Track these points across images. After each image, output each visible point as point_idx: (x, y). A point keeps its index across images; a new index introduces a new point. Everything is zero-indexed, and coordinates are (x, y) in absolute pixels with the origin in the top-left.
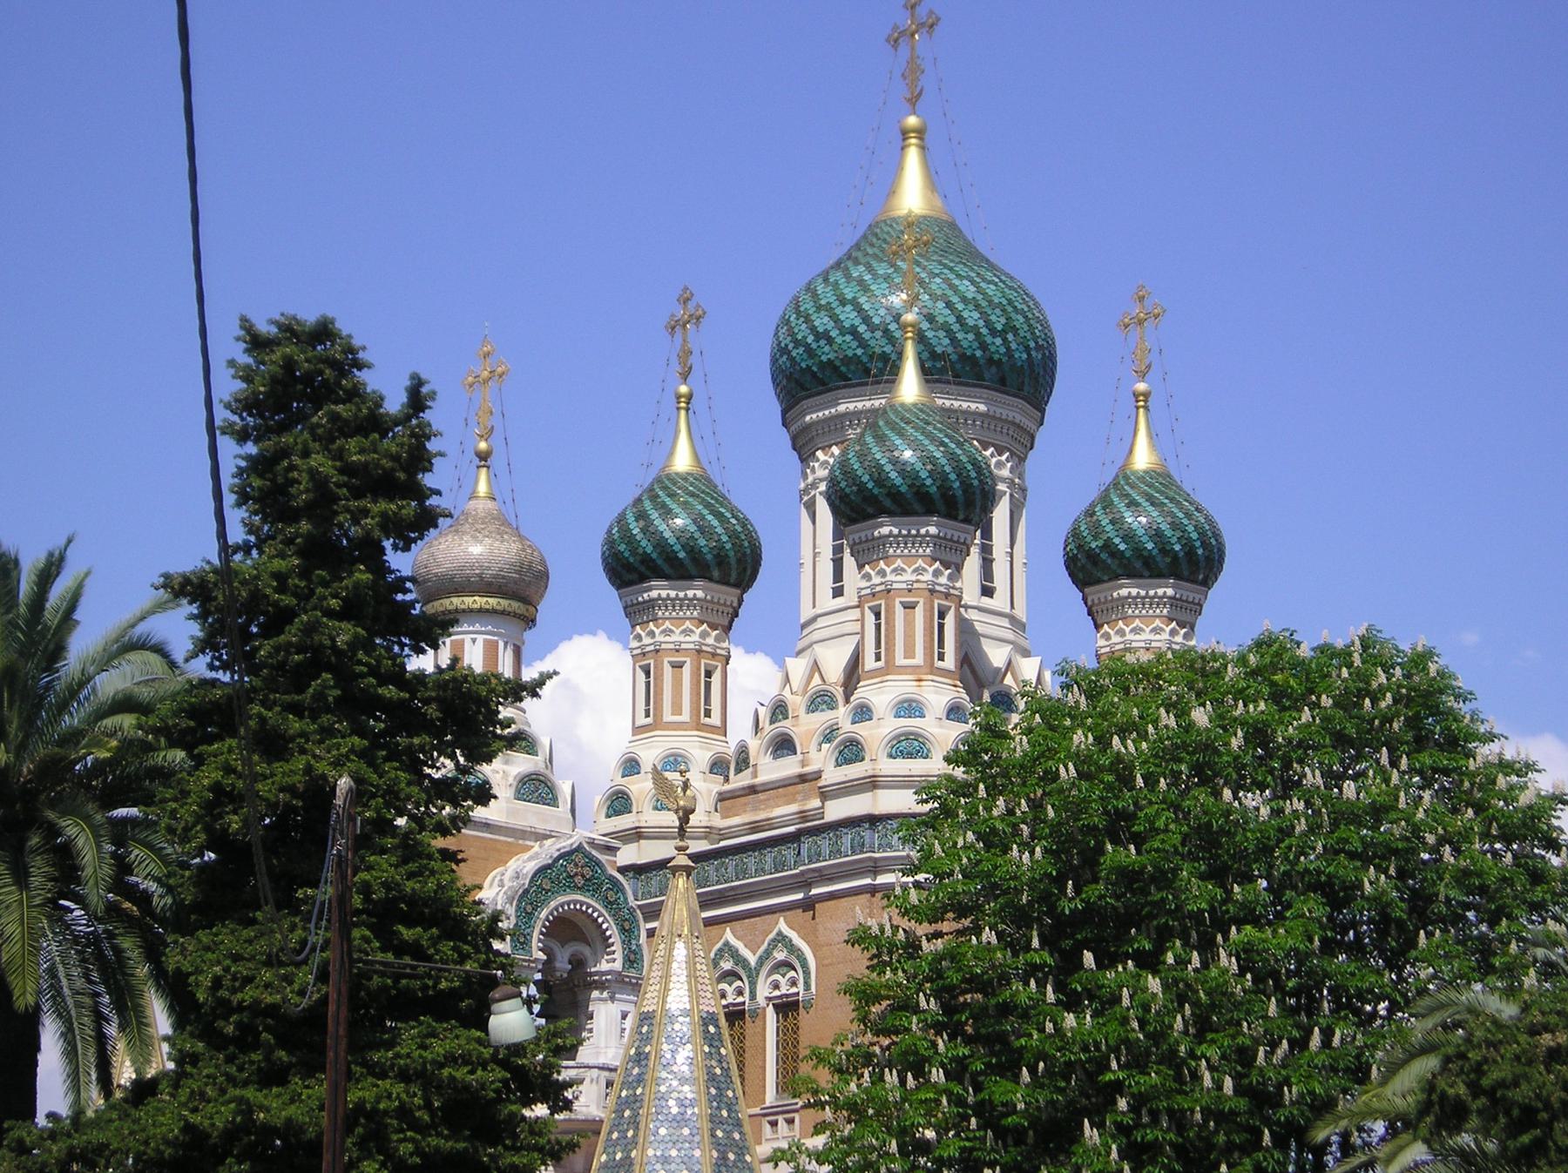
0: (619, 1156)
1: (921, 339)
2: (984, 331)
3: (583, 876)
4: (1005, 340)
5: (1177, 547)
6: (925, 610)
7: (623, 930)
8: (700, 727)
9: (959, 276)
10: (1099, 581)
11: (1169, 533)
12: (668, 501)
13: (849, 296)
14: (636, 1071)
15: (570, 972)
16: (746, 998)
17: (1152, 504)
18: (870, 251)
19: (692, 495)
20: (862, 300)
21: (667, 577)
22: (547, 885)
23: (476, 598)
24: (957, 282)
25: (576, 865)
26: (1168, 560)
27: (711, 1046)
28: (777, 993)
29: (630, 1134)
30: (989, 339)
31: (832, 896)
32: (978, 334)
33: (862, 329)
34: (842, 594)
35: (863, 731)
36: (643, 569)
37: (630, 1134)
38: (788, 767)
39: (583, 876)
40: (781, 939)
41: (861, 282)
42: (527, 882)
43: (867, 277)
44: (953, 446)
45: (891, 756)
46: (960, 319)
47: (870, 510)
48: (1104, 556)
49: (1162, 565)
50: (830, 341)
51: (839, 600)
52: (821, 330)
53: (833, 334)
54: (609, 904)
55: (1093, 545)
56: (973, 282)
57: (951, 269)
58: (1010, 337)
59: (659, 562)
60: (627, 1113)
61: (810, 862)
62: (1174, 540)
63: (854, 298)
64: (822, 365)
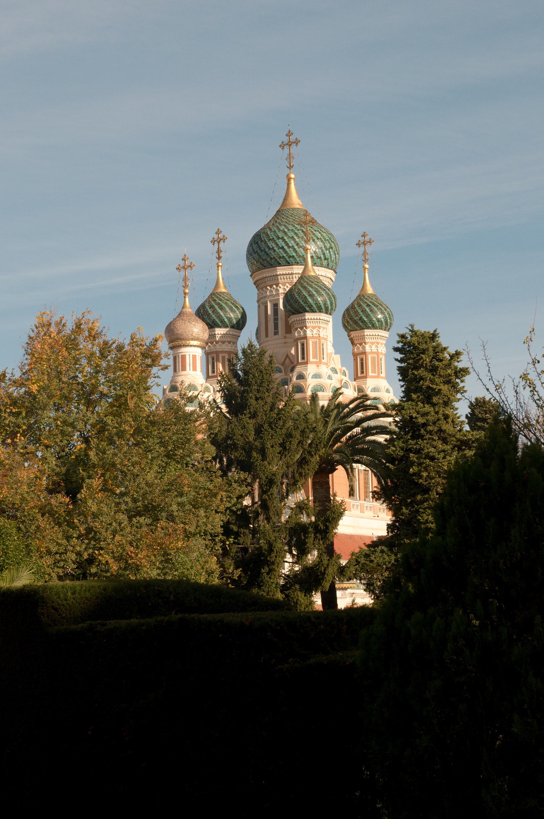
2: (324, 249)
4: (330, 252)
9: (315, 230)
12: (220, 302)
13: (281, 236)
17: (375, 306)
18: (284, 220)
19: (228, 300)
20: (285, 238)
21: (220, 327)
24: (315, 232)
30: (325, 251)
32: (322, 251)
33: (286, 247)
41: (284, 232)
43: (286, 230)
44: (327, 291)
47: (301, 311)
49: (378, 325)
50: (275, 251)
52: (271, 247)
53: (276, 249)
55: (356, 319)
56: (320, 233)
57: (312, 228)
58: (331, 250)
63: (283, 237)
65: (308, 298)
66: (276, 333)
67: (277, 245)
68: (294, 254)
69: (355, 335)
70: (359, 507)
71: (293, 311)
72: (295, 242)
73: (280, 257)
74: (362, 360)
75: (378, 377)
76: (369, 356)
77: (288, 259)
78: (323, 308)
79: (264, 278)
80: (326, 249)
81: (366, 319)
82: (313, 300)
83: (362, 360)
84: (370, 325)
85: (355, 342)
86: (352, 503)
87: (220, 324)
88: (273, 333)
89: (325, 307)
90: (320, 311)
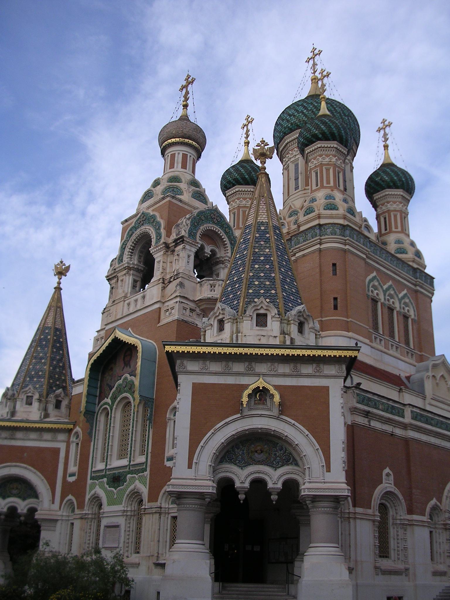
3: (217, 219)
4: (348, 119)
5: (404, 179)
6: (333, 170)
7: (231, 243)
10: (379, 191)
11: (401, 175)
15: (210, 255)
21: (242, 184)
22: (202, 217)
23: (181, 139)
25: (214, 215)
26: (401, 183)
27: (277, 237)
30: (344, 117)
31: (304, 256)
32: (341, 115)
35: (314, 205)
36: (234, 182)
39: (217, 219)
42: (195, 214)
45: (325, 209)
46: (335, 109)
47: (314, 140)
49: (399, 185)
50: (294, 116)
54: (226, 233)
55: (377, 179)
58: (350, 118)
59: (240, 179)
61: (296, 245)
62: (403, 177)
65: (320, 125)
66: (297, 188)
67: (297, 111)
69: (377, 197)
70: (383, 342)
72: (314, 106)
74: (385, 219)
76: (392, 213)
78: (338, 137)
80: (345, 115)
83: (385, 219)
84: (392, 184)
85: (378, 204)
86: (374, 335)
87: (241, 181)
88: (294, 190)
89: (339, 135)
90: (334, 140)
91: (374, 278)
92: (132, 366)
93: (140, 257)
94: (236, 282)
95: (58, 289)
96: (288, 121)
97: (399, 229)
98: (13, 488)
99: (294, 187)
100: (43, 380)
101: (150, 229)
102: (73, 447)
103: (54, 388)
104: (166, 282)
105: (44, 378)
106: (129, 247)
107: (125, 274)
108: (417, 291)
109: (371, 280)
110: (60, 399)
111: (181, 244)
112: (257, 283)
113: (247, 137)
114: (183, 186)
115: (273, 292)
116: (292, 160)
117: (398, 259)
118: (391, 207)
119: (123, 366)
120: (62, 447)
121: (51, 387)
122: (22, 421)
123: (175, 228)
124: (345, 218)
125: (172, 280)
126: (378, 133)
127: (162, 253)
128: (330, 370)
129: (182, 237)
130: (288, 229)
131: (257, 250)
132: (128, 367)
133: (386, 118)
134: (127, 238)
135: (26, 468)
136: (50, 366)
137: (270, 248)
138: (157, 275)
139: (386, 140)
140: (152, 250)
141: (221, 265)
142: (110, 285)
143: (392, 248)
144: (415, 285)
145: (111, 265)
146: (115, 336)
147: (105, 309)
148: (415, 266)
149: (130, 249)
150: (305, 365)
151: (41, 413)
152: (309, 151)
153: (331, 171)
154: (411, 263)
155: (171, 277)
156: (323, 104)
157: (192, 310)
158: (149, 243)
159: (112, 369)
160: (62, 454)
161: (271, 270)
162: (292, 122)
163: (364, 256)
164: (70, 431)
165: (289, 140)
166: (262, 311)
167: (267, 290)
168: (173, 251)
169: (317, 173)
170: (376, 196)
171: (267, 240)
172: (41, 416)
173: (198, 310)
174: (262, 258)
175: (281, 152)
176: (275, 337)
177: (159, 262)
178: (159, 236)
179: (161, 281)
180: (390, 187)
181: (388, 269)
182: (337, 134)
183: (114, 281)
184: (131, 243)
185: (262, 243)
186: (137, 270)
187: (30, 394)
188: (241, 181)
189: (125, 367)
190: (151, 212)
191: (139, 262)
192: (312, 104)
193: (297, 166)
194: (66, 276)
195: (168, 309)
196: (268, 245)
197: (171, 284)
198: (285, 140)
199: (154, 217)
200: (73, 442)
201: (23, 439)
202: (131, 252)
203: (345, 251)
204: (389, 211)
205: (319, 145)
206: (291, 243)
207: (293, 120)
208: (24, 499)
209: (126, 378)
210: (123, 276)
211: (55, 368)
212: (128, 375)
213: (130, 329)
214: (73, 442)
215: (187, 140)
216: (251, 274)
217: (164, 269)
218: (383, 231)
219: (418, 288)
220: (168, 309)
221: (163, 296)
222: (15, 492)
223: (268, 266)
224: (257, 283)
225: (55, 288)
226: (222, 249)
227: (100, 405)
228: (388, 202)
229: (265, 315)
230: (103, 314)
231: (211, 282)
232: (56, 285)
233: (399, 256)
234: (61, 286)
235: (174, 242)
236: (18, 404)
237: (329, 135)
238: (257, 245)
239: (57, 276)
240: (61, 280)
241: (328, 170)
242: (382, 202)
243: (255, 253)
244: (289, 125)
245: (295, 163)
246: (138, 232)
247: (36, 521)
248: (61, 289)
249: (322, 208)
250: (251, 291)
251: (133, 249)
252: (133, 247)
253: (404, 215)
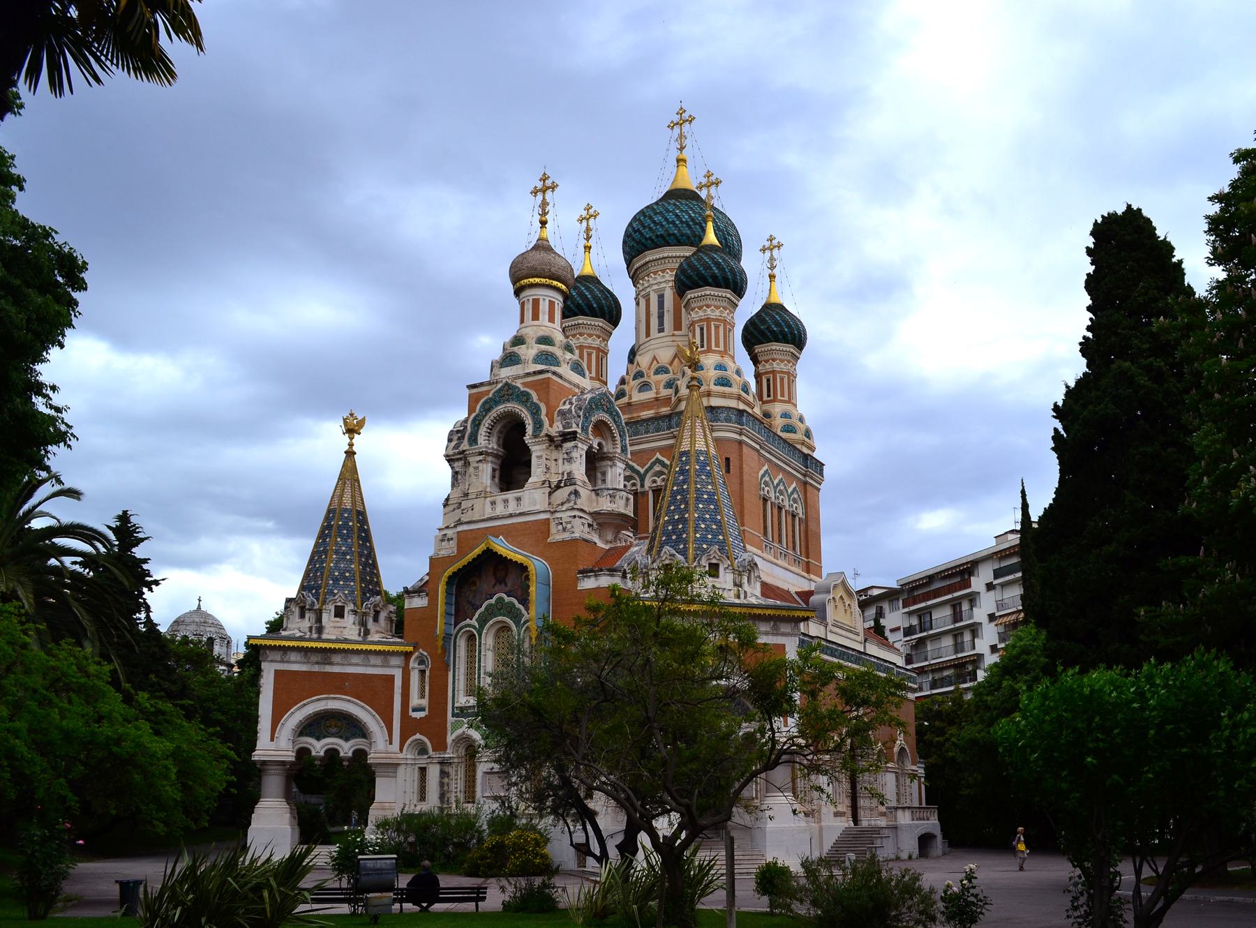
0: (676, 517)
1: (714, 221)
8: (599, 380)
14: (681, 478)
15: (598, 450)
16: (639, 487)
21: (587, 316)
28: (655, 485)
29: (682, 506)
33: (677, 222)
34: (663, 331)
36: (576, 310)
37: (682, 506)
38: (649, 395)
40: (658, 461)
45: (715, 384)
47: (701, 284)
48: (767, 332)
50: (662, 226)
51: (662, 334)
53: (664, 223)
54: (615, 422)
59: (585, 307)
60: (679, 497)
64: (657, 236)
66: (661, 330)
67: (666, 219)
68: (689, 232)
69: (760, 350)
71: (690, 284)
72: (690, 216)
73: (670, 235)
74: (768, 380)
75: (789, 401)
77: (680, 238)
78: (732, 284)
79: (647, 263)
81: (775, 329)
82: (718, 268)
87: (587, 310)
89: (733, 280)
91: (766, 472)
92: (509, 585)
93: (499, 437)
94: (679, 521)
95: (350, 454)
96: (651, 229)
97: (786, 398)
98: (331, 727)
99: (657, 327)
100: (352, 584)
101: (521, 411)
102: (415, 678)
103: (368, 595)
104: (553, 486)
105: (353, 581)
106: (487, 425)
107: (480, 461)
108: (805, 483)
109: (763, 476)
110: (378, 609)
111: (571, 441)
112: (703, 526)
113: (588, 238)
114: (557, 351)
115: (721, 537)
116: (655, 287)
117: (785, 441)
118: (776, 366)
119: (493, 583)
120: (398, 675)
121: (364, 594)
122: (337, 641)
123: (558, 416)
124: (739, 398)
125: (562, 485)
126: (761, 254)
127: (544, 446)
128: (785, 628)
129: (575, 432)
130: (657, 393)
131: (699, 486)
132: (503, 585)
133: (774, 235)
134: (480, 411)
135: (349, 701)
136: (360, 564)
137: (713, 484)
138: (537, 474)
139: (772, 267)
140: (528, 439)
141: (609, 463)
142: (452, 468)
143: (778, 422)
144: (805, 475)
145: (450, 440)
146: (488, 548)
147: (447, 499)
148: (805, 451)
149: (488, 428)
150: (764, 623)
151: (360, 630)
152: (693, 296)
153: (721, 329)
154: (799, 446)
155: (560, 482)
156: (710, 227)
157: (590, 525)
158: (524, 432)
159: (474, 583)
160: (398, 683)
161: (718, 510)
162: (659, 233)
163: (758, 447)
164: (407, 655)
165: (651, 258)
166: (714, 561)
167: (715, 536)
168: (561, 447)
169: (702, 329)
170: (758, 349)
171: (709, 475)
172: (360, 632)
173: (595, 526)
174: (705, 496)
175: (636, 270)
176: (730, 590)
177: (539, 457)
178: (538, 425)
179: (547, 484)
180: (777, 341)
181: (779, 459)
182: (731, 281)
183: (458, 465)
184: (489, 421)
185: (703, 477)
186: (496, 456)
187: (339, 604)
188: (587, 310)
189: (498, 585)
190: (519, 385)
191: (499, 445)
192: (687, 212)
193: (661, 298)
194: (359, 434)
195: (562, 523)
196: (710, 481)
197: (559, 491)
198: (645, 256)
199: (527, 395)
200: (413, 668)
201: (343, 665)
202: (489, 433)
203: (740, 443)
204: (773, 372)
205: (708, 293)
206: (670, 420)
207: (660, 231)
208: (347, 740)
209: (501, 599)
210: (477, 462)
211: (364, 568)
212: (504, 596)
213: (501, 537)
214: (413, 668)
215: (555, 283)
216: (696, 515)
217: (548, 469)
218: (765, 398)
219: (808, 479)
220: (562, 523)
221: (550, 504)
222: (334, 730)
223: (712, 507)
224: (703, 526)
225: (345, 452)
226: (610, 443)
227: (458, 627)
228: (774, 360)
229: (717, 565)
230: (445, 506)
231: (611, 492)
232: (347, 447)
233: (784, 435)
234: (354, 448)
235: (560, 436)
236: (325, 617)
237: (721, 281)
238: (698, 480)
239: (347, 435)
240: (353, 441)
241: (717, 327)
242: (765, 358)
243: (697, 490)
244: (653, 237)
245: (662, 293)
246: (501, 408)
247: (370, 765)
248: (355, 453)
249: (712, 383)
250: (698, 535)
251: (491, 428)
252: (492, 426)
253: (791, 377)
